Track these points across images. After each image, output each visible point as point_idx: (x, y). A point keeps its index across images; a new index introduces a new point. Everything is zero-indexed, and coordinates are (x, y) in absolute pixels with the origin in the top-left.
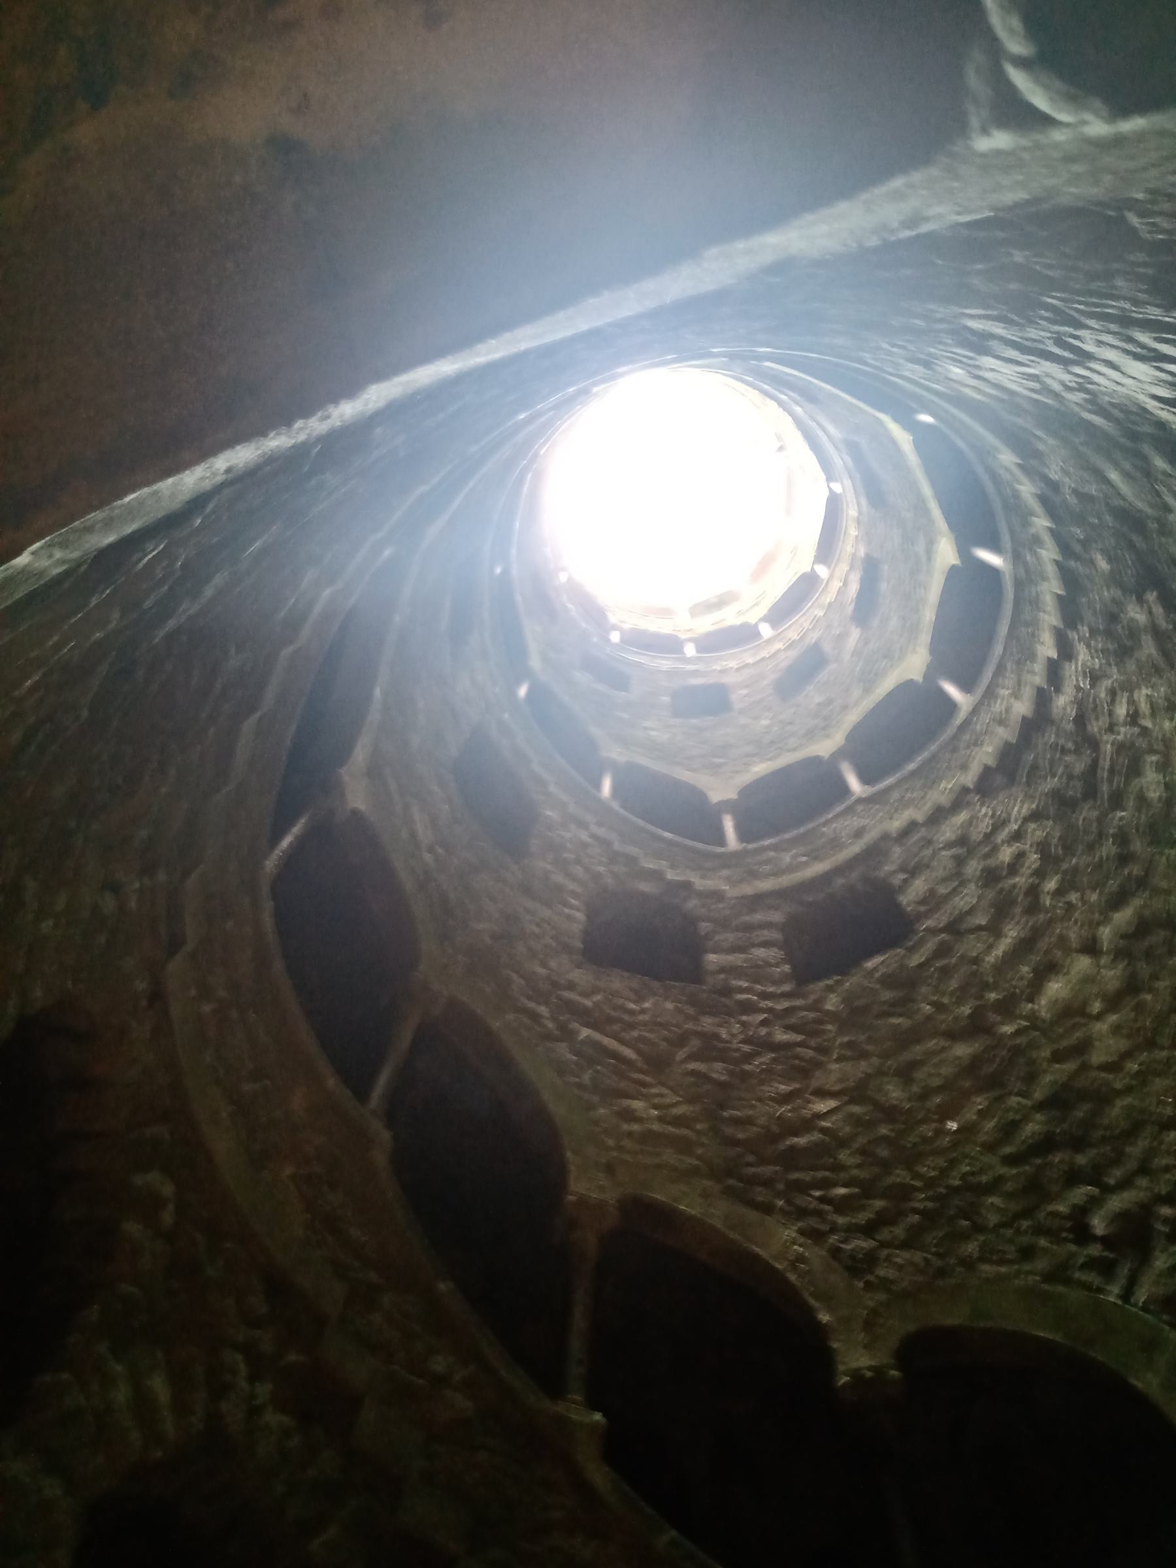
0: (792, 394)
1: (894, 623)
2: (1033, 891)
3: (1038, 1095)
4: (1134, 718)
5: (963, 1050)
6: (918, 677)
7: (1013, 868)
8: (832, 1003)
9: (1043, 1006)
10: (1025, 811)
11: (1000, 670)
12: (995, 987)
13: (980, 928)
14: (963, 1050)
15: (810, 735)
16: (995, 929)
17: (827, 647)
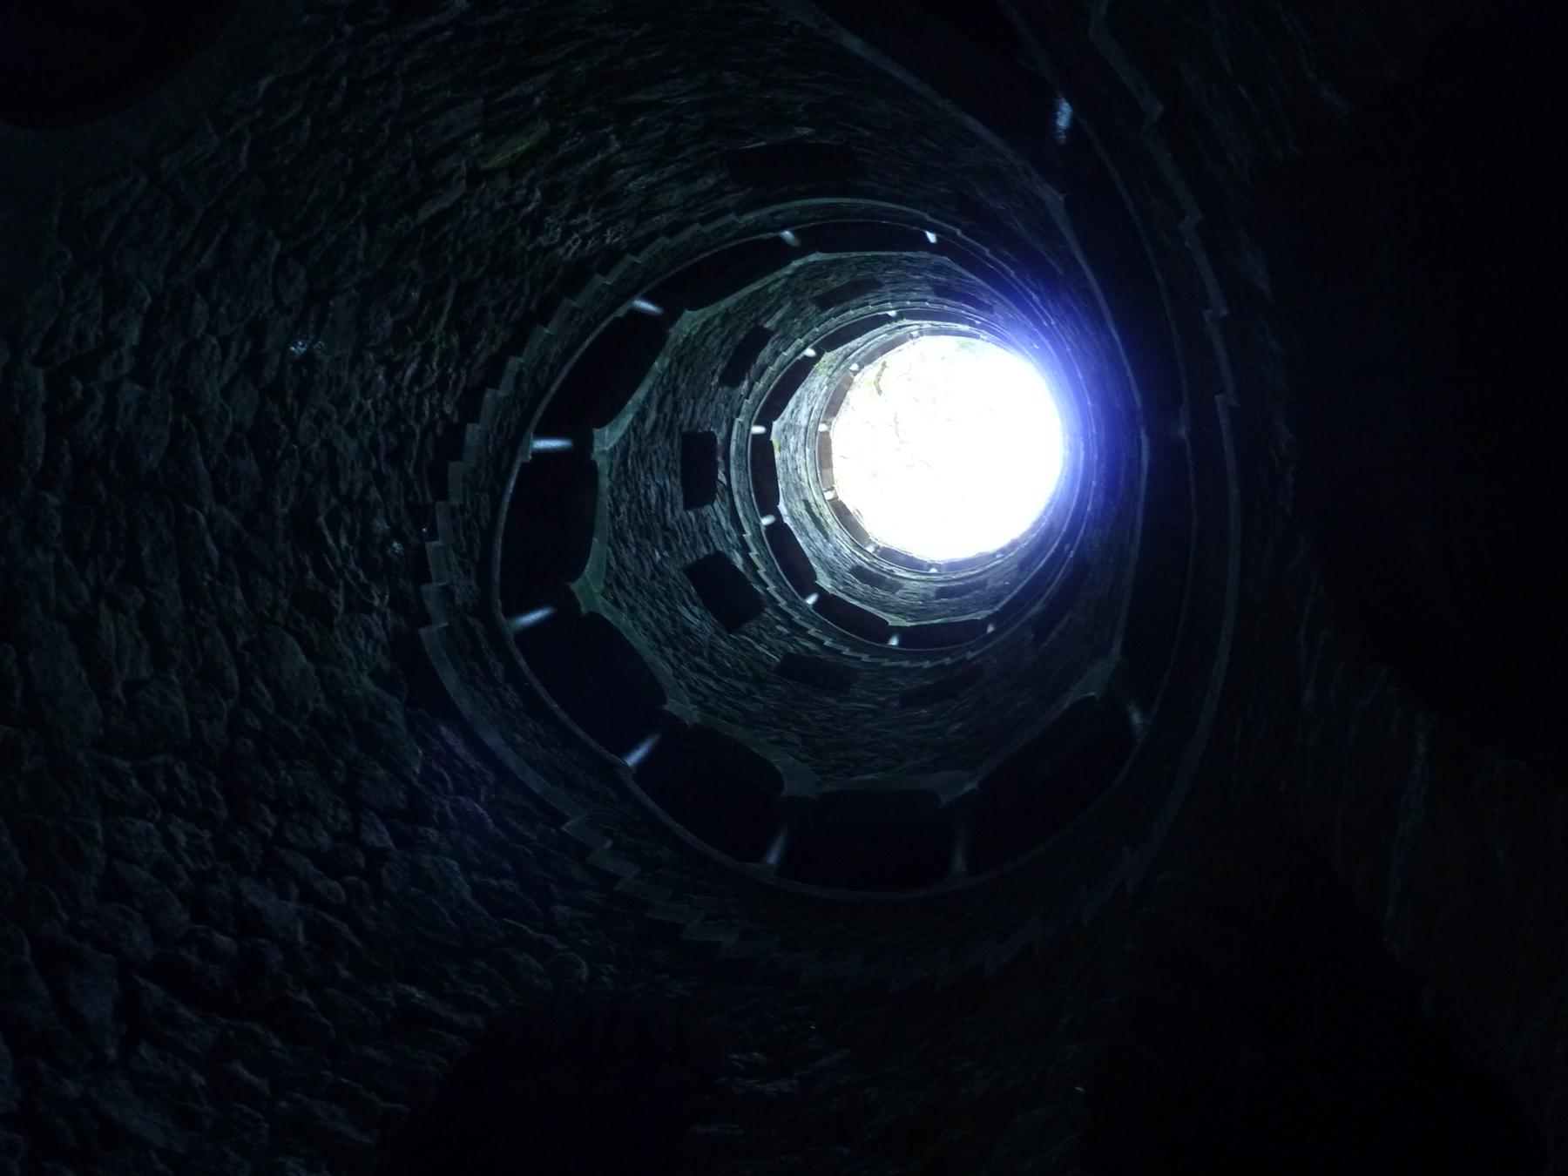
0: (738, 560)
1: (713, 342)
2: (551, 196)
3: (544, 77)
4: (393, 369)
5: (640, 96)
6: (688, 313)
7: (580, 208)
8: (807, 131)
9: (543, 127)
10: (561, 251)
11: (569, 352)
12: (607, 135)
13: (623, 166)
14: (640, 96)
15: (834, 262)
16: (606, 169)
17: (812, 308)
